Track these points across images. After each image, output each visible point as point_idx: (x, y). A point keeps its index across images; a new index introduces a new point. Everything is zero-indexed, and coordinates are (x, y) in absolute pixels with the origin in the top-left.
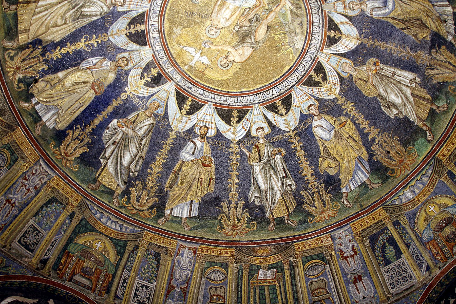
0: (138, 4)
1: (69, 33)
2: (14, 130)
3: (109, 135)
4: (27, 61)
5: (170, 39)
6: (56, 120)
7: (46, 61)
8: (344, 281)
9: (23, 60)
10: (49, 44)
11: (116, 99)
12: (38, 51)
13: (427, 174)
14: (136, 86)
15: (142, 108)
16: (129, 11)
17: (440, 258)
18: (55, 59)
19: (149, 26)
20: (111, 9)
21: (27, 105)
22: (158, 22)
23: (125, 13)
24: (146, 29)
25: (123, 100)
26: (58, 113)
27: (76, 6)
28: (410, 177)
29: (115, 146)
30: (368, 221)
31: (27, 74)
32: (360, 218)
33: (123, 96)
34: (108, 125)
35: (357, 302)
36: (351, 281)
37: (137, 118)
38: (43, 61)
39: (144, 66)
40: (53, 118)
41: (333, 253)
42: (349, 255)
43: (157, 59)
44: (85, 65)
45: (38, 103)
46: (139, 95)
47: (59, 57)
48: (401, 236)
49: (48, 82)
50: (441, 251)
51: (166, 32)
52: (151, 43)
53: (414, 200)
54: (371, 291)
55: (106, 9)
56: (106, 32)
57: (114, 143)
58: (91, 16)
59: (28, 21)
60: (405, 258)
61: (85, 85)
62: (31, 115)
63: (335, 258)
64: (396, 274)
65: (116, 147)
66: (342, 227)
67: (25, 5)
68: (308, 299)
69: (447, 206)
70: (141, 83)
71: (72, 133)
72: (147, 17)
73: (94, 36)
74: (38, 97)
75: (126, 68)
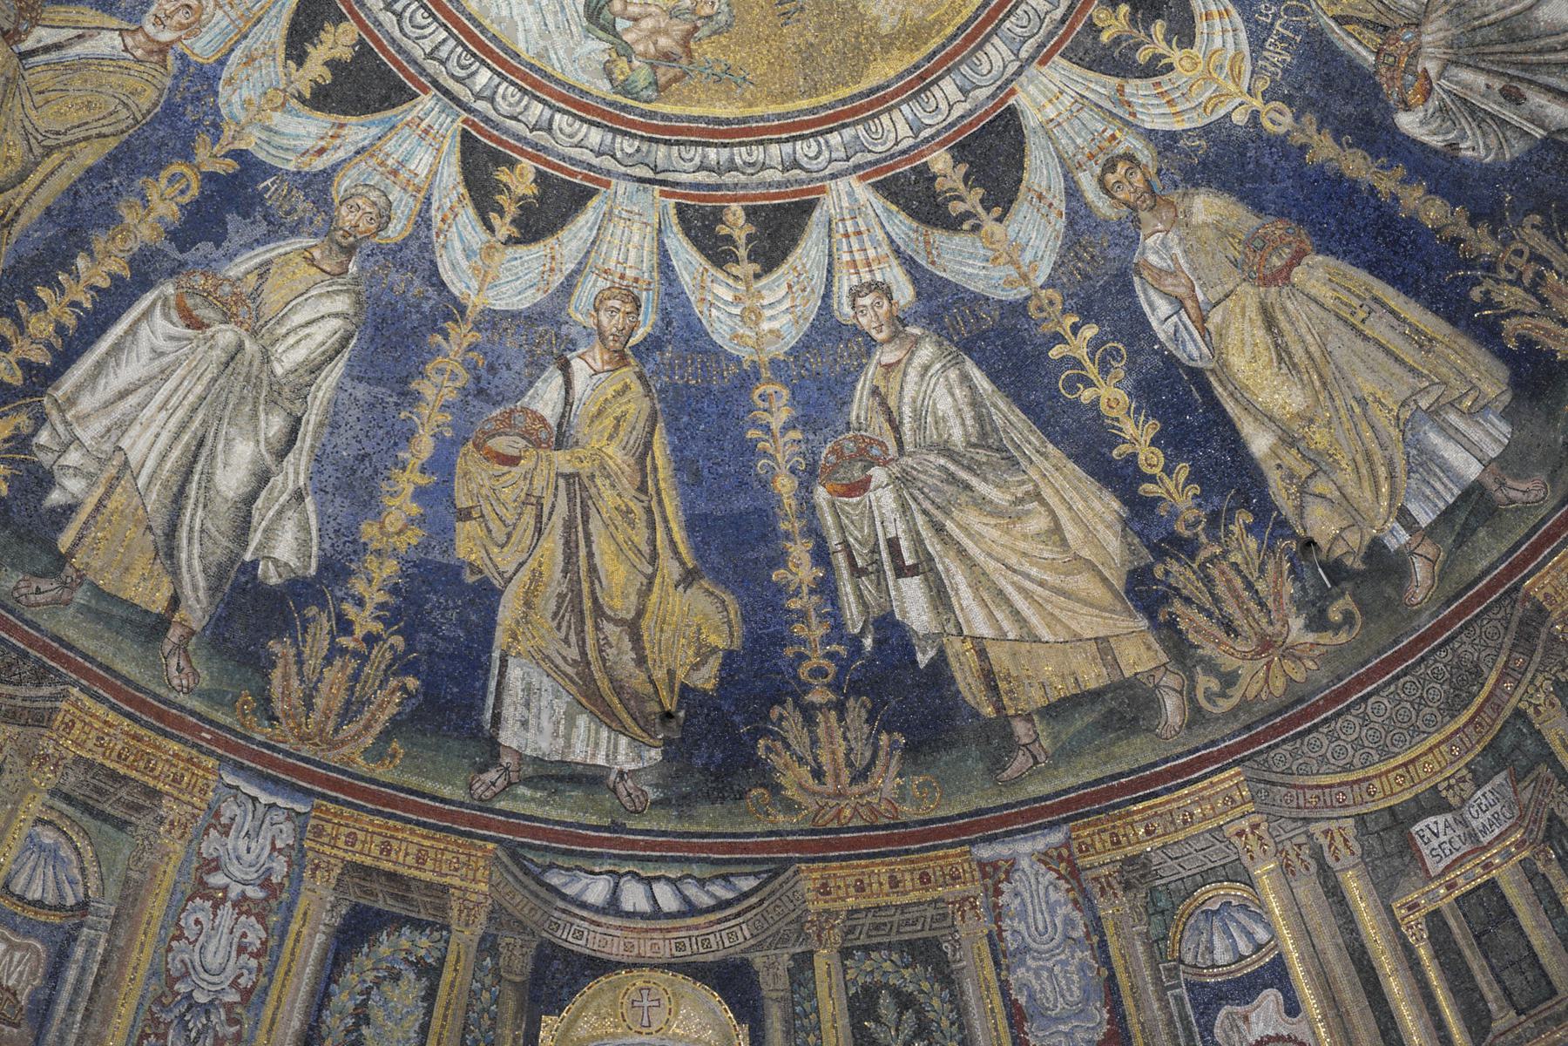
0: (850, 230)
1: (1071, 465)
2: (1540, 609)
3: (1484, 134)
4: (1231, 608)
5: (936, 21)
6: (1469, 414)
7: (1214, 519)
9: (1229, 627)
10: (1139, 534)
11: (1303, 148)
12: (1179, 573)
14: (1208, 78)
15: (1302, 10)
16: (897, 251)
18: (1195, 489)
19: (926, 140)
20: (917, 331)
21: (1420, 570)
22: (889, 110)
23: (910, 265)
24: (942, 144)
25: (1297, 119)
26: (1433, 413)
27: (952, 479)
29: (1523, 88)
31: (1286, 599)
33: (1278, 120)
34: (1436, 152)
37: (1359, 21)
38: (1218, 539)
39: (1105, 78)
40: (1462, 426)
43: (1051, 35)
44: (1190, 347)
45: (1404, 516)
46: (1246, 48)
47: (1182, 480)
49: (1303, 490)
51: (918, 56)
52: (993, 96)
55: (926, 352)
56: (1018, 309)
57: (1513, 97)
58: (976, 403)
59: (1064, 652)
61: (1281, 317)
62: (1461, 540)
65: (1530, 82)
67: (1003, 686)
70: (1186, 63)
71: (1514, 320)
72: (891, 168)
73: (1055, 352)
74: (1379, 524)
75: (1145, 154)
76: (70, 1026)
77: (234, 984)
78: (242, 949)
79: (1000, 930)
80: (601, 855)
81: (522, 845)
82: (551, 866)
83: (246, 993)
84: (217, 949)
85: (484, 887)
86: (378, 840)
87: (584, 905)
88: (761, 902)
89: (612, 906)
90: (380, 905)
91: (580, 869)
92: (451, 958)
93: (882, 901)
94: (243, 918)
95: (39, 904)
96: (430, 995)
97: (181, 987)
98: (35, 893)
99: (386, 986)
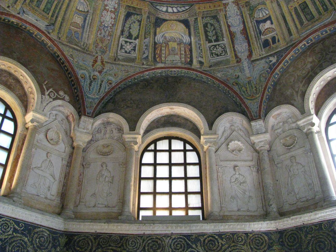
76: (87, 29)
77: (111, 23)
78: (112, 18)
79: (226, 14)
80: (165, 4)
81: (153, 2)
82: (157, 5)
83: (113, 25)
84: (108, 18)
85: (147, 9)
86: (131, 2)
87: (162, 11)
88: (190, 10)
89: (167, 11)
90: (132, 11)
91: (162, 6)
92: (143, 19)
93: (208, 10)
94: (111, 14)
95: (81, 11)
96: (140, 25)
97: (103, 24)
98: (81, 9)
99: (133, 23)
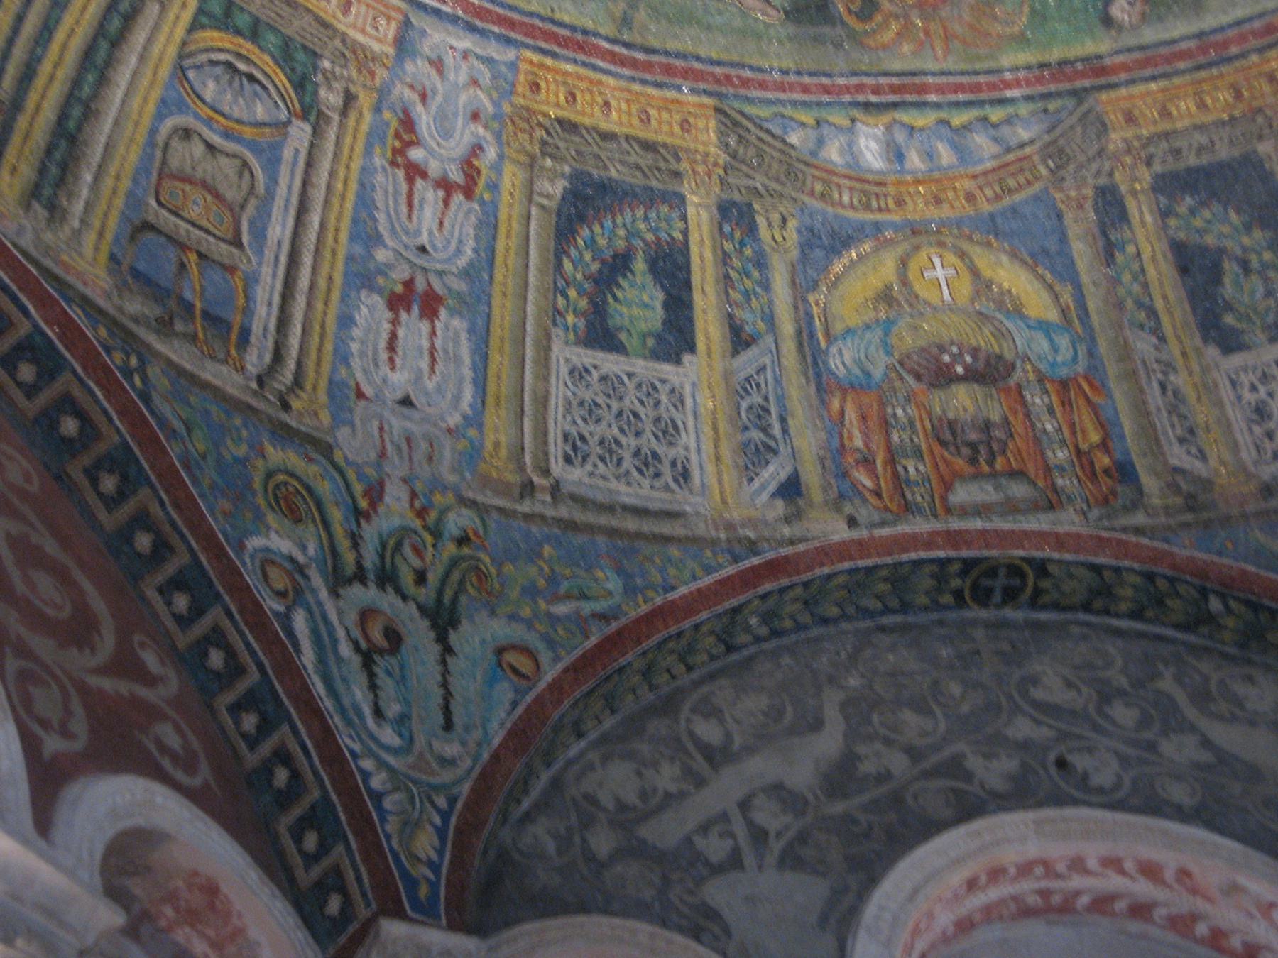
8: (350, 259)
13: (1005, 131)
17: (868, 483)
28: (923, 89)
30: (612, 104)
32: (584, 64)
35: (360, 395)
36: (381, 281)
41: (365, 100)
42: (434, 168)
48: (727, 277)
50: (891, 461)
53: (880, 184)
54: (457, 399)
60: (700, 377)
63: (365, 127)
64: (620, 413)
66: (482, 33)
68: (126, 184)
69: (1018, 312)
